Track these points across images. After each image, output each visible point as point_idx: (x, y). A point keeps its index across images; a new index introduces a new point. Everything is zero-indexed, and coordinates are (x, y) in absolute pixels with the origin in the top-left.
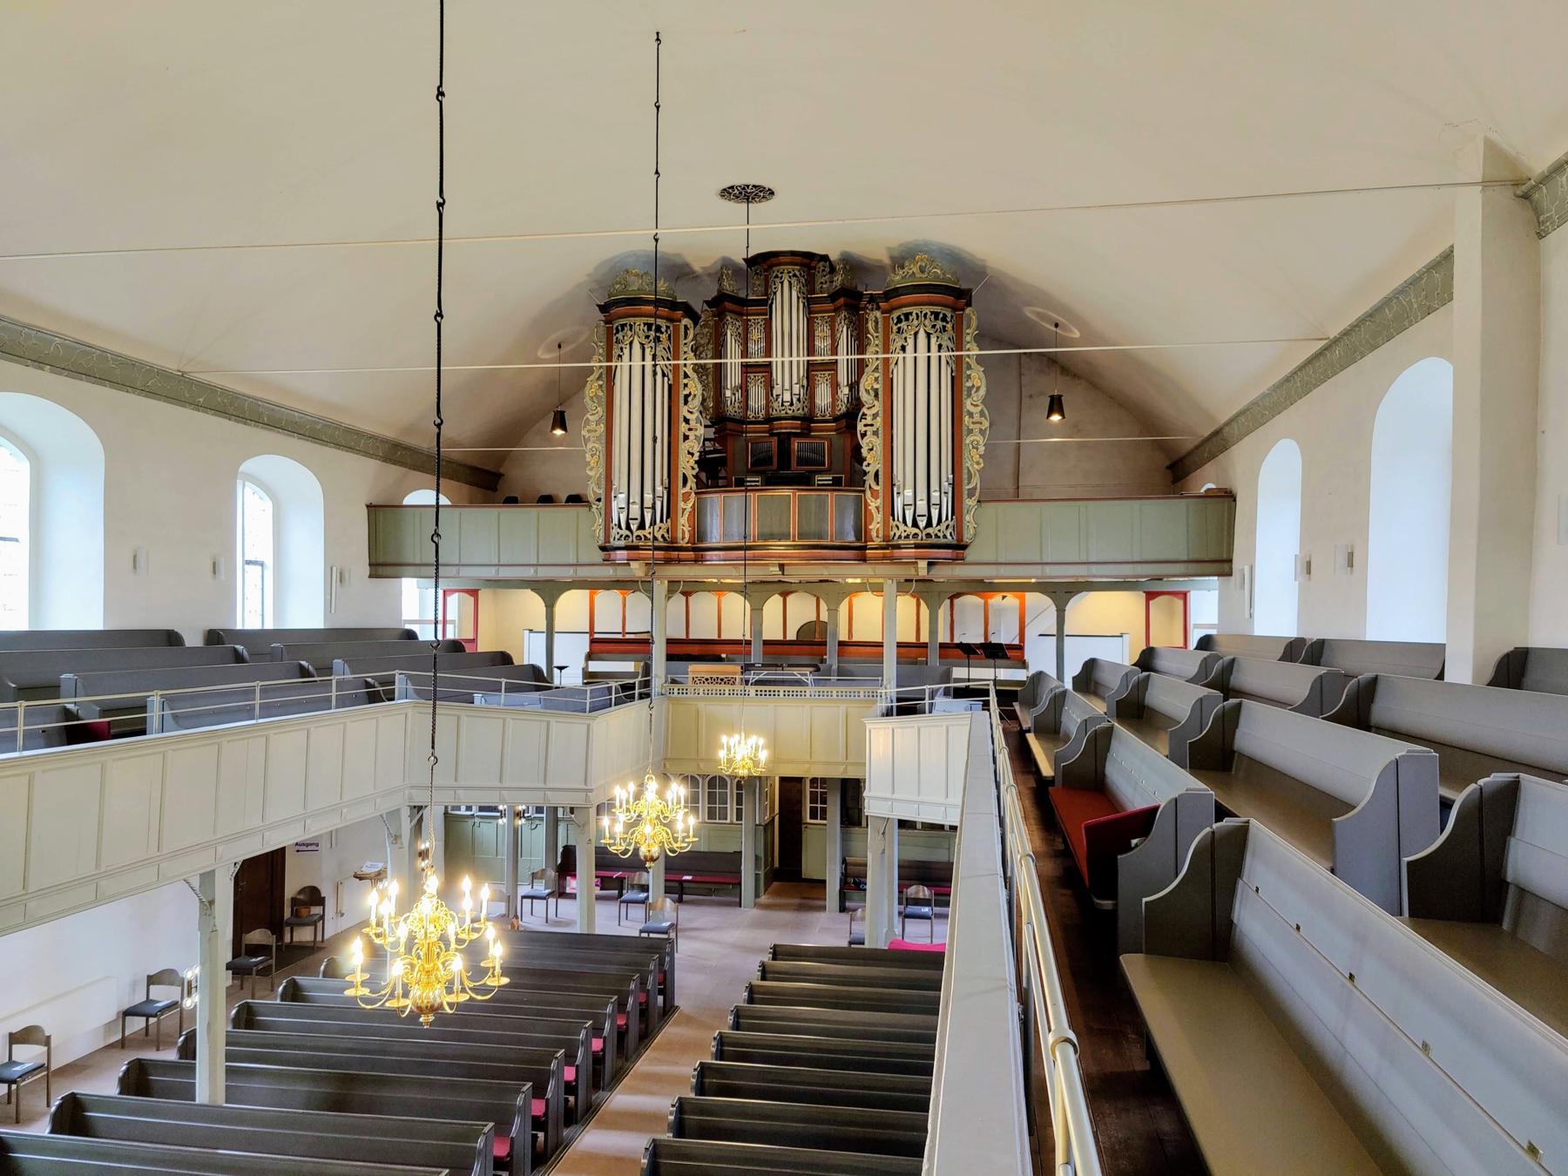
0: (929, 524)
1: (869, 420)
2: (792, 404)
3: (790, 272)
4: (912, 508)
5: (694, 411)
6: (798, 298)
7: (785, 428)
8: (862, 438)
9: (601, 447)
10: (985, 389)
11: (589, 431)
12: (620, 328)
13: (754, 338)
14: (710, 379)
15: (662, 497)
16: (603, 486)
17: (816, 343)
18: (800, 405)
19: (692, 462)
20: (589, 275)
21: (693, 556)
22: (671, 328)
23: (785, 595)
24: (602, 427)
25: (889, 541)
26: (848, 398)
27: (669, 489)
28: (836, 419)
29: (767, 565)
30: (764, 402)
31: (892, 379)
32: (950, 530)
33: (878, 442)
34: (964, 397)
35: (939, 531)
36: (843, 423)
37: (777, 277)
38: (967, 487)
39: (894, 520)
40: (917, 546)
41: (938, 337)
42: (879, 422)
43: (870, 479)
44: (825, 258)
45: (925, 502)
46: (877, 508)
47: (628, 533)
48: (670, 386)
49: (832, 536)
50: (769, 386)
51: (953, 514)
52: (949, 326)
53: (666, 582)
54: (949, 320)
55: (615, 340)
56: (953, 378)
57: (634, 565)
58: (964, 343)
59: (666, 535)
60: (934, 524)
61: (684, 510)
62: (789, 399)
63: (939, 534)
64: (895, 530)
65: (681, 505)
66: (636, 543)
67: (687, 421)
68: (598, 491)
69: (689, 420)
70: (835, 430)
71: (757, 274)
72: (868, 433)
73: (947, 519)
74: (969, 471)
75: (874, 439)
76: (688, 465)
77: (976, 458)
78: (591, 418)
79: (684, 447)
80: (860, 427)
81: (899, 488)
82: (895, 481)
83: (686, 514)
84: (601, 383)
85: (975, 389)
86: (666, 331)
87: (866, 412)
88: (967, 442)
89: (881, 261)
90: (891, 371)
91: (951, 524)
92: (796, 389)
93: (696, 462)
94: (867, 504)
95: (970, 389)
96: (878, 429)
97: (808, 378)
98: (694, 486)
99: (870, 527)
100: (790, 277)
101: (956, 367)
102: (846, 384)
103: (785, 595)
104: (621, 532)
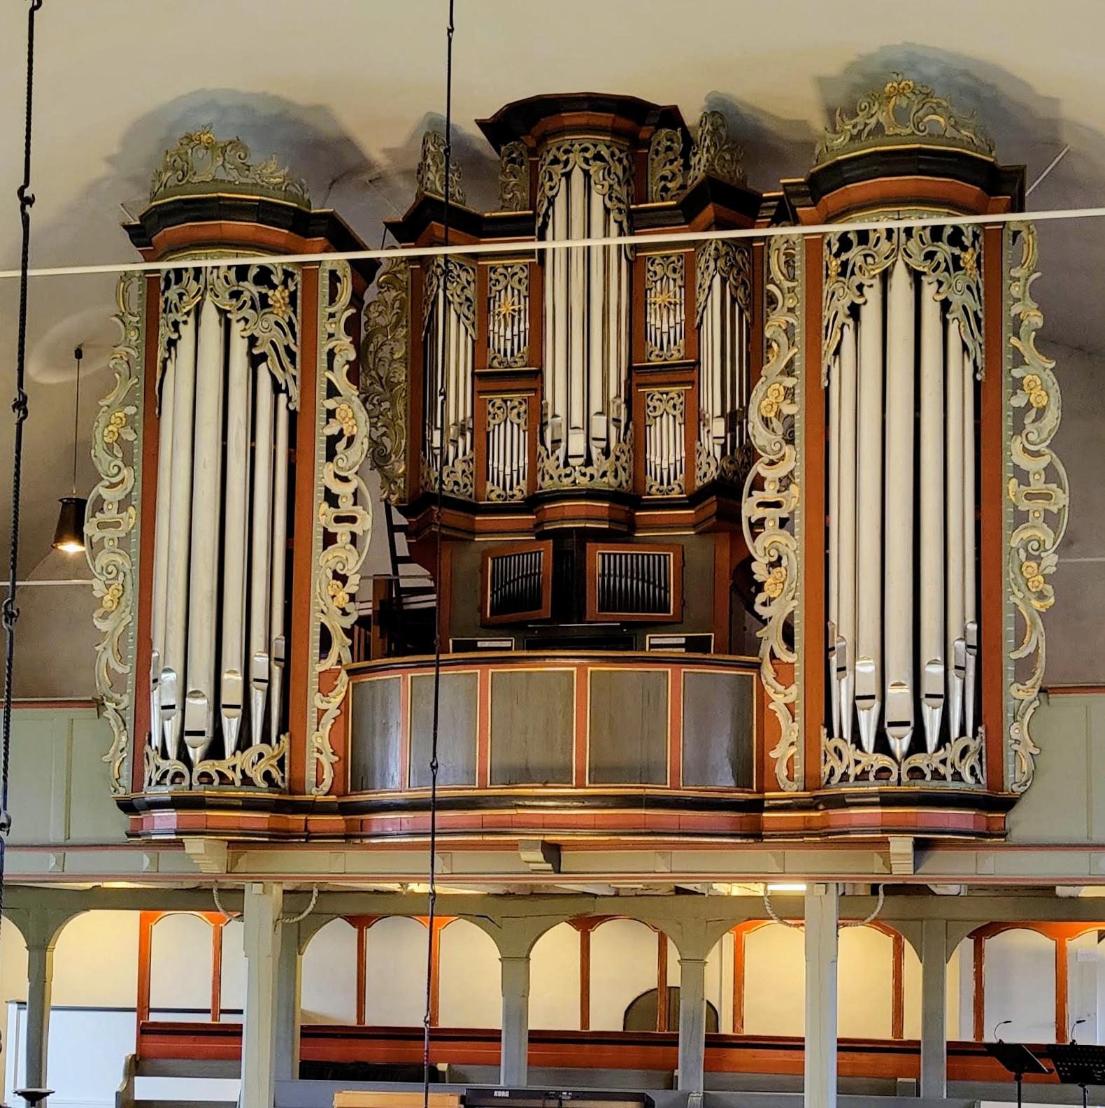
0: (918, 744)
1: (770, 494)
2: (589, 462)
3: (586, 150)
4: (876, 704)
5: (350, 474)
6: (607, 211)
7: (573, 519)
8: (754, 536)
9: (127, 563)
10: (1058, 413)
11: (101, 526)
12: (172, 276)
13: (503, 310)
14: (400, 408)
15: (269, 681)
16: (132, 656)
17: (651, 320)
18: (607, 465)
19: (342, 597)
20: (111, 160)
21: (342, 826)
22: (298, 278)
23: (585, 924)
24: (132, 517)
25: (819, 789)
26: (724, 447)
27: (287, 664)
28: (695, 499)
29: (514, 846)
30: (524, 461)
31: (827, 389)
32: (971, 760)
33: (792, 546)
34: (1007, 432)
35: (943, 762)
36: (711, 505)
37: (556, 161)
38: (1014, 656)
39: (830, 735)
40: (887, 800)
41: (940, 284)
42: (794, 498)
43: (771, 638)
44: (671, 117)
45: (907, 691)
46: (790, 707)
47: (181, 767)
48: (292, 415)
49: (675, 774)
50: (537, 421)
51: (978, 721)
52: (968, 258)
53: (277, 891)
54: (967, 242)
55: (162, 305)
56: (977, 385)
57: (194, 845)
58: (1007, 302)
59: (276, 774)
60: (931, 746)
62: (582, 451)
63: (942, 770)
64: (833, 761)
65: (316, 701)
66: (199, 790)
67: (332, 499)
68: (120, 669)
69: (337, 496)
70: (694, 526)
71: (513, 161)
72: (769, 524)
73: (963, 732)
74: (1018, 615)
75: (782, 537)
76: (333, 606)
77: (1038, 582)
78: (107, 494)
79: (323, 561)
80: (749, 509)
81: (842, 657)
82: (835, 642)
83: (328, 721)
84: (131, 410)
85: (1033, 413)
86: (285, 283)
87: (763, 474)
88: (1015, 543)
89: (803, 125)
90: (824, 370)
91: (974, 745)
92: (599, 426)
94: (764, 699)
95: (1020, 413)
96: (792, 513)
97: (628, 402)
98: (346, 656)
99: (773, 754)
100: (586, 161)
101: (987, 359)
102: (718, 412)
103: (585, 924)
104: (165, 765)
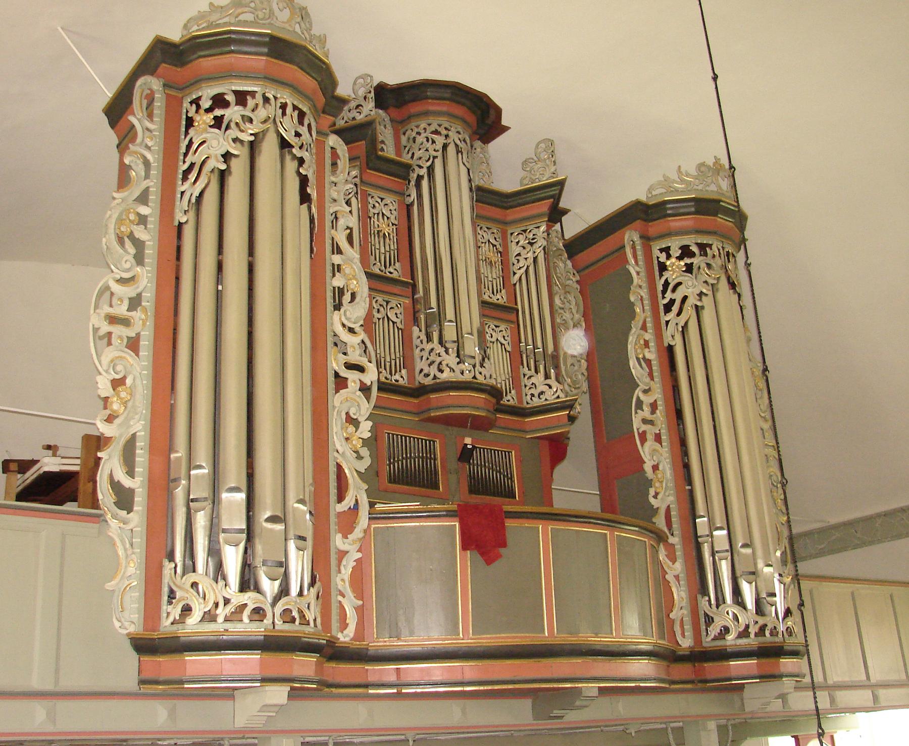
61: (342, 554)
93: (365, 442)
